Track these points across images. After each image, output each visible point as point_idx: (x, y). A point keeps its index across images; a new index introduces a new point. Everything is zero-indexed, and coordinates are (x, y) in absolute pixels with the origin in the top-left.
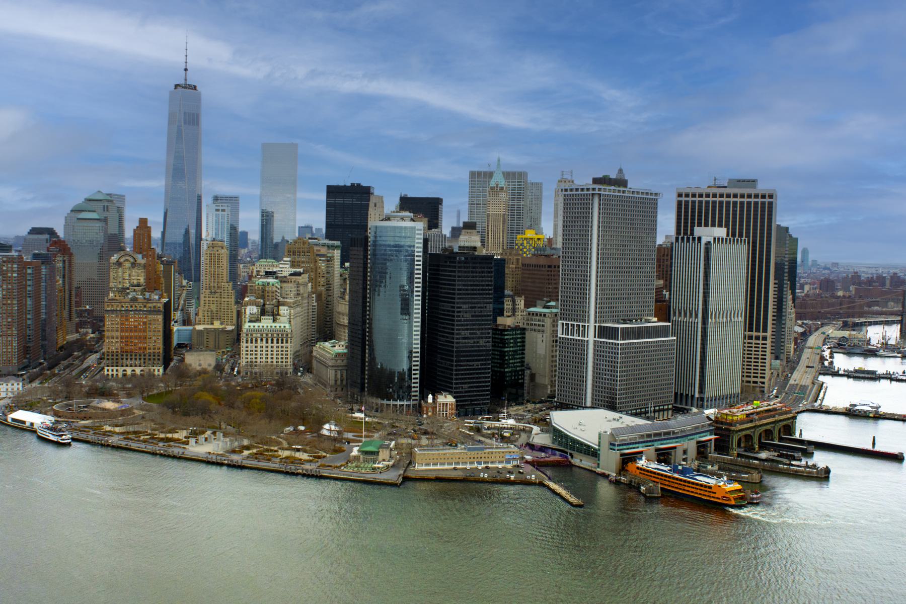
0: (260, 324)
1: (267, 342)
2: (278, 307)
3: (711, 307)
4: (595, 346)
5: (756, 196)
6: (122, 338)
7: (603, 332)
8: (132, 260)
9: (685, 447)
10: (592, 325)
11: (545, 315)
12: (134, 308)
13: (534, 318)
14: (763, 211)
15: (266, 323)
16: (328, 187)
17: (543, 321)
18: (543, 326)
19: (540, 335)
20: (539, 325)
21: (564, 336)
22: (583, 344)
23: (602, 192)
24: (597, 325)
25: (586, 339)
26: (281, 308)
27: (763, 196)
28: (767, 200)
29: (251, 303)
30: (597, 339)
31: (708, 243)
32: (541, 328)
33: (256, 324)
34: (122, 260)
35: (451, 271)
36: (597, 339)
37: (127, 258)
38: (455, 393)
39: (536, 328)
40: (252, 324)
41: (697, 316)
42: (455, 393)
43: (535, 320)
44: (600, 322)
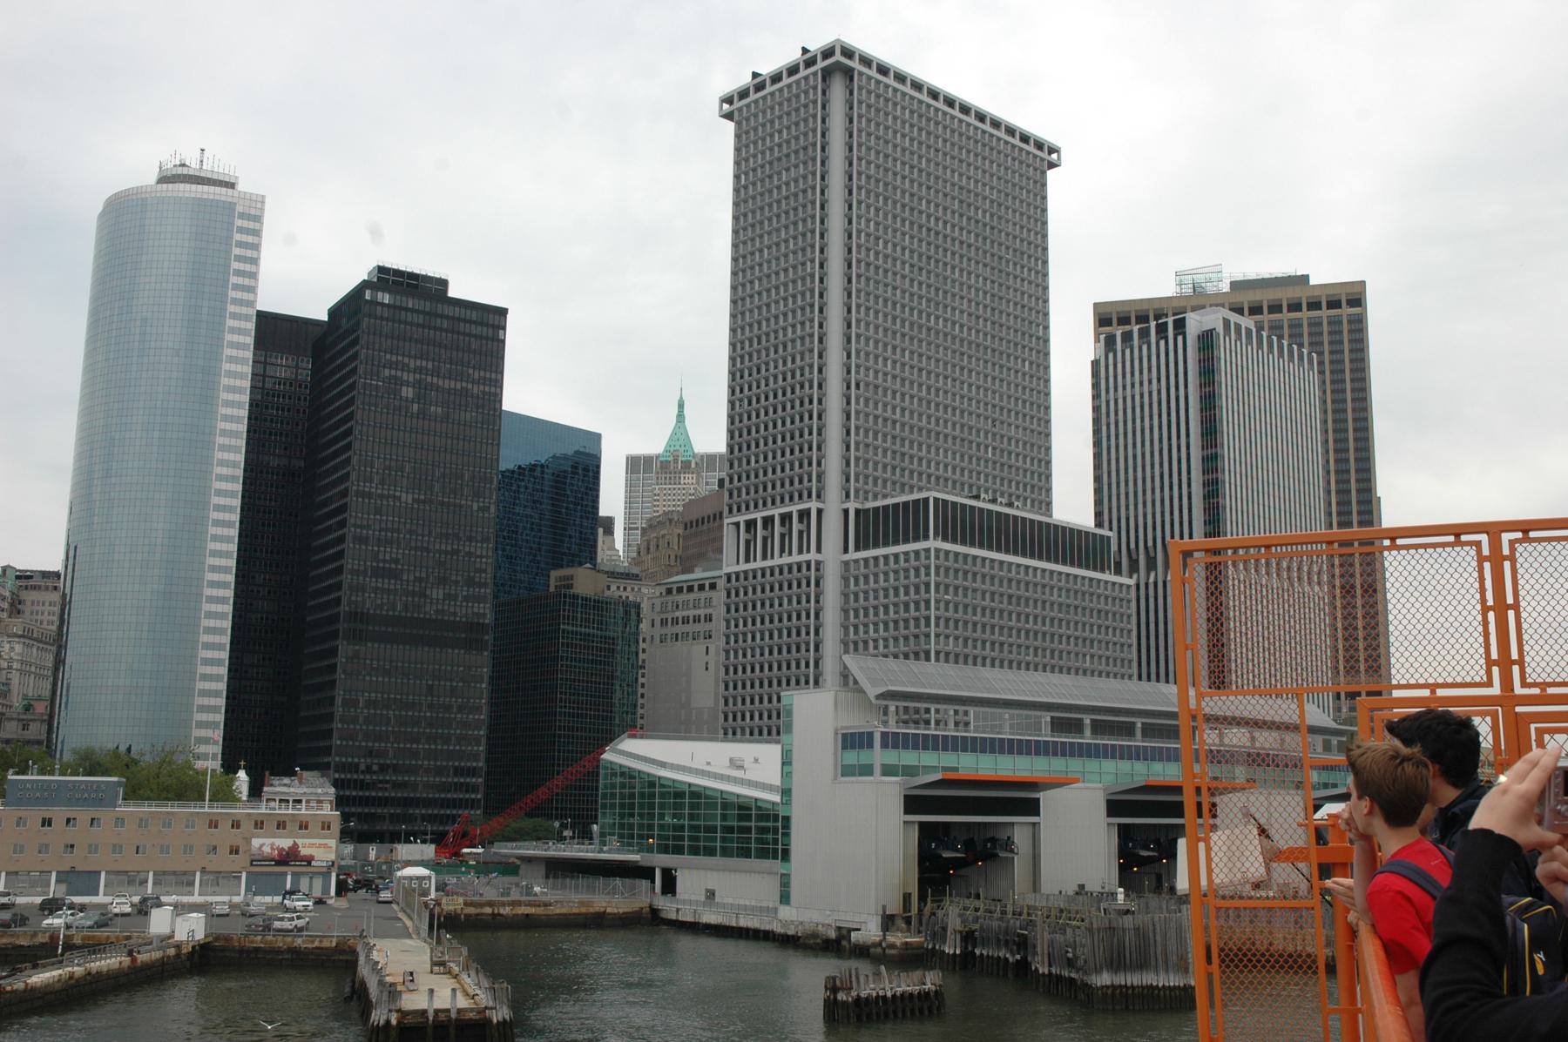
5: (1314, 305)
7: (873, 527)
18: (709, 618)
19: (698, 648)
20: (697, 619)
22: (808, 578)
24: (852, 506)
25: (812, 556)
27: (1334, 304)
28: (1346, 311)
30: (853, 555)
31: (1207, 340)
32: (701, 627)
36: (853, 555)
38: (341, 768)
42: (341, 768)
43: (686, 604)
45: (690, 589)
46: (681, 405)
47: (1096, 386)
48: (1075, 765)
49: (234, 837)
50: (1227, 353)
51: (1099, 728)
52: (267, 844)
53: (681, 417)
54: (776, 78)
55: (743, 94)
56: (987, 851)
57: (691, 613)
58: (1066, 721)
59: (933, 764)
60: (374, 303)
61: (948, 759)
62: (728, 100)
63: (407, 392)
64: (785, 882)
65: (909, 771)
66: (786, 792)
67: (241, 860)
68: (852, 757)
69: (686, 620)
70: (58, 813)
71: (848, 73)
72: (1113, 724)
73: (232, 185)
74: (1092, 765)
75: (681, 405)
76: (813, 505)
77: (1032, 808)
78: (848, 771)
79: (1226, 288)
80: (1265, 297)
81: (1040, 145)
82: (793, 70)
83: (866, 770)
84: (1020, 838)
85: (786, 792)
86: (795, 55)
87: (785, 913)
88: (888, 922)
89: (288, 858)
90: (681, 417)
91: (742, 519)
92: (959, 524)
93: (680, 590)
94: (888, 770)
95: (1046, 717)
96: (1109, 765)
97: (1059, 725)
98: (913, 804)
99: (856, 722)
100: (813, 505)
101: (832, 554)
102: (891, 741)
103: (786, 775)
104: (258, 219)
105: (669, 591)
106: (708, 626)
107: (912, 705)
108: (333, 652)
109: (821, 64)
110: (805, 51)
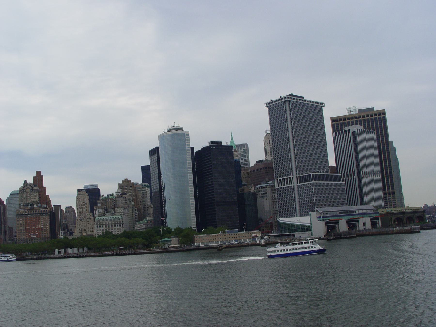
0: (104, 217)
1: (109, 226)
2: (114, 208)
3: (361, 168)
4: (298, 188)
5: (375, 115)
6: (26, 230)
7: (302, 179)
8: (31, 188)
9: (364, 221)
10: (295, 176)
11: (266, 187)
12: (32, 213)
13: (260, 190)
14: (380, 122)
15: (108, 217)
16: (142, 167)
17: (266, 190)
18: (266, 193)
19: (265, 199)
20: (264, 194)
21: (279, 187)
23: (290, 99)
24: (298, 176)
25: (292, 185)
26: (116, 209)
27: (379, 114)
28: (382, 116)
29: (99, 208)
30: (299, 184)
31: (354, 133)
32: (265, 195)
33: (102, 217)
34: (25, 188)
35: (210, 166)
37: (28, 187)
39: (263, 195)
40: (100, 218)
41: (354, 175)
43: (261, 191)
44: (299, 174)
45: (262, 188)
46: (232, 136)
47: (334, 142)
48: (342, 217)
49: (250, 235)
50: (358, 135)
51: (344, 213)
52: (253, 235)
53: (232, 138)
54: (275, 101)
55: (269, 103)
56: (334, 228)
57: (263, 192)
58: (340, 212)
59: (328, 219)
60: (213, 148)
61: (329, 218)
62: (267, 104)
63: (220, 163)
64: (312, 233)
65: (325, 220)
66: (311, 224)
67: (251, 237)
68: (319, 219)
69: (262, 194)
70: (233, 234)
71: (289, 101)
72: (346, 212)
73: (182, 129)
74: (344, 217)
75: (232, 136)
76: (291, 176)
77: (338, 223)
78: (318, 221)
79: (357, 113)
80: (365, 114)
81: (321, 104)
82: (279, 100)
83: (321, 220)
84: (337, 226)
85: (311, 224)
86: (279, 98)
87: (312, 237)
88: (325, 236)
89: (256, 236)
90: (232, 138)
91: (278, 179)
92: (317, 178)
93: (260, 188)
94: (323, 220)
95: (338, 212)
96: (346, 217)
97: (340, 213)
98: (326, 223)
99: (319, 215)
100: (291, 176)
101: (295, 183)
102: (323, 217)
103: (311, 221)
104: (189, 135)
105: (257, 189)
106: (266, 195)
107: (325, 213)
108: (215, 208)
109: (284, 100)
110: (281, 97)
